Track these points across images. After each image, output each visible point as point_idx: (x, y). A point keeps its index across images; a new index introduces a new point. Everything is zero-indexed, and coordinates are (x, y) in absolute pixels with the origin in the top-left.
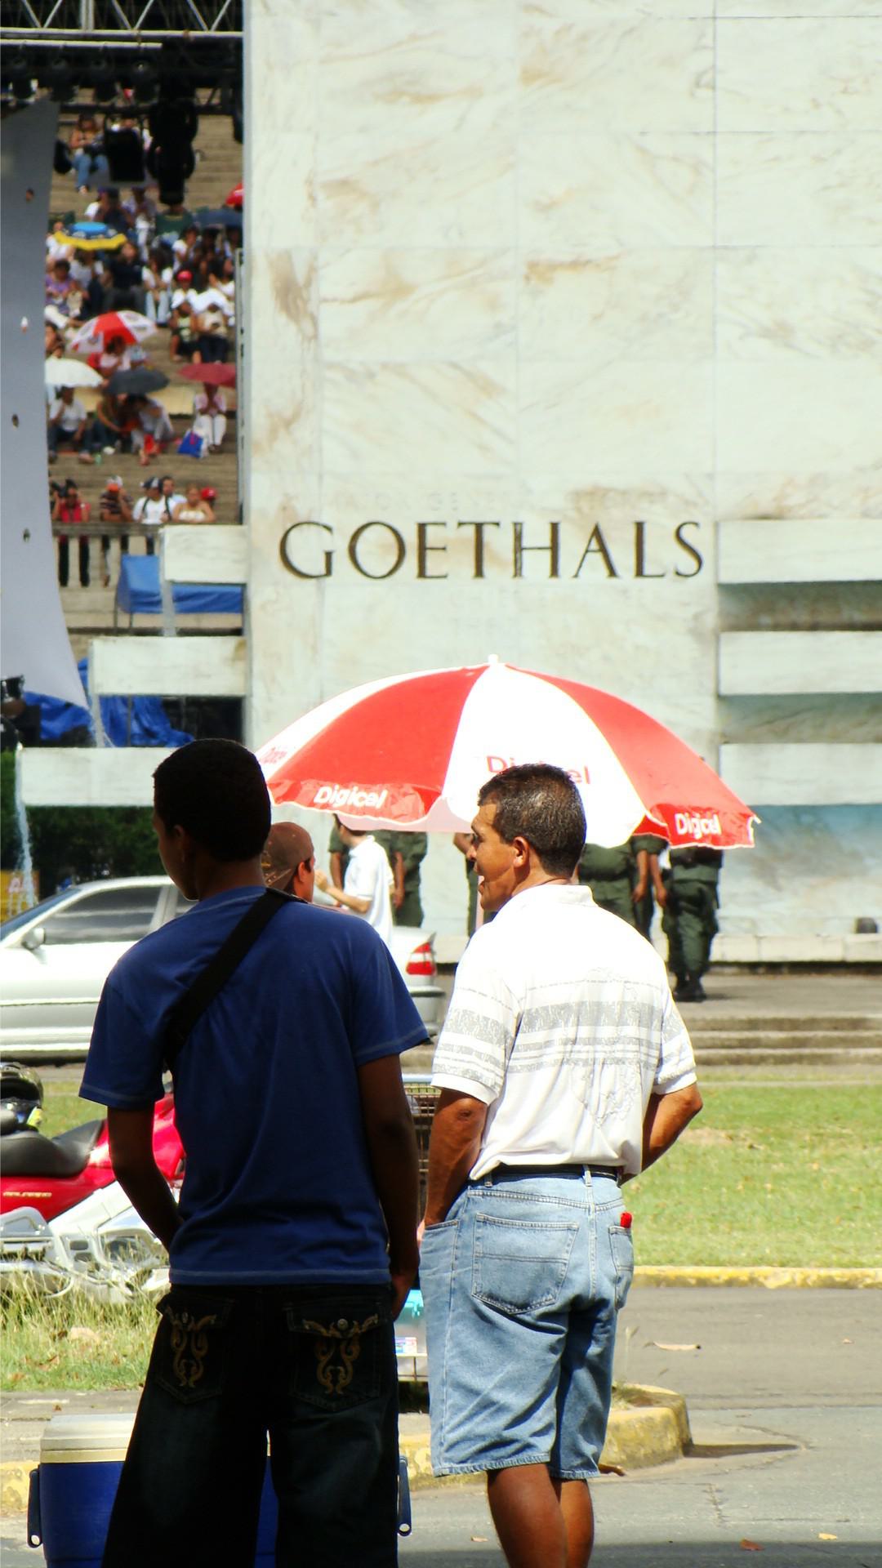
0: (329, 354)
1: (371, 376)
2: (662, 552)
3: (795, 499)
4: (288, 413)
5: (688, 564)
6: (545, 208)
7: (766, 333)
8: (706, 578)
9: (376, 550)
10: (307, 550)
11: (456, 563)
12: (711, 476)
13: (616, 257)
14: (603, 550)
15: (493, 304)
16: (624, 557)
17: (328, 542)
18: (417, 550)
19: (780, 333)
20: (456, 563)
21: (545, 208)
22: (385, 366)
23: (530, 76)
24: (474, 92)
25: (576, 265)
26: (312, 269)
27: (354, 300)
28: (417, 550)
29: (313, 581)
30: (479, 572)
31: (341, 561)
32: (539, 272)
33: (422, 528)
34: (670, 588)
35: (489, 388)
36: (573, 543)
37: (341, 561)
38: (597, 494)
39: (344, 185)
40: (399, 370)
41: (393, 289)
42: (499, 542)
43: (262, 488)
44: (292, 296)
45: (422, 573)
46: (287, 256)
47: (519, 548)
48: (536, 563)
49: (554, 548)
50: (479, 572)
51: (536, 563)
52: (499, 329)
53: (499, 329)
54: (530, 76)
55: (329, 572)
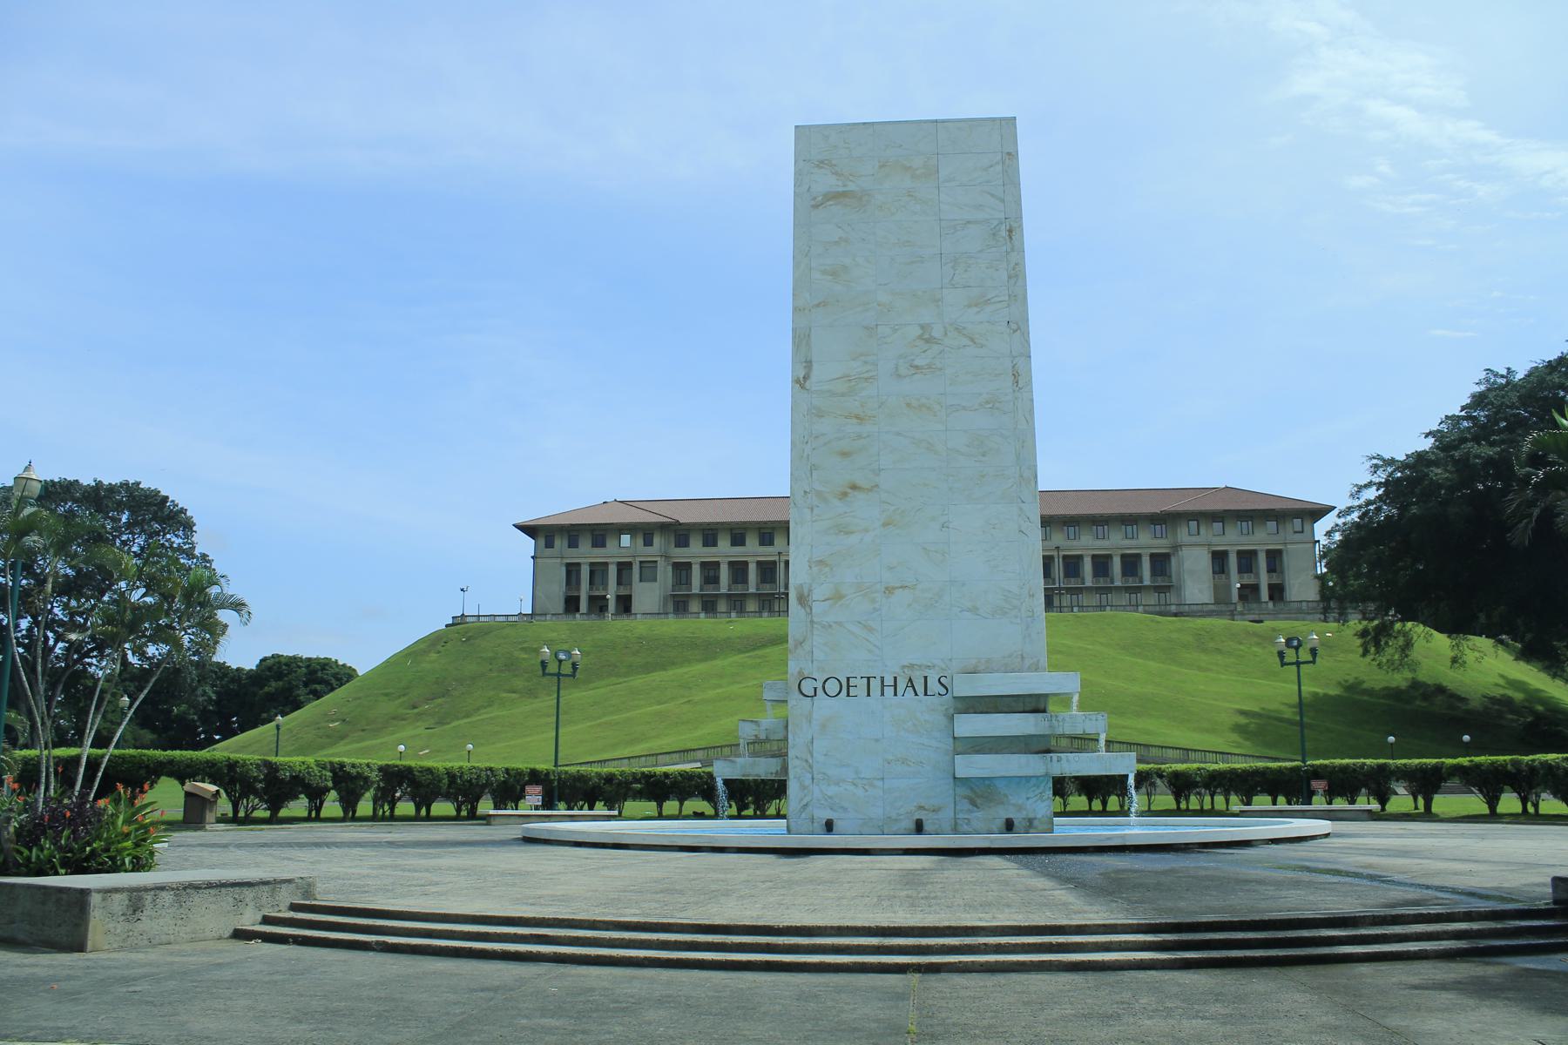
2: (934, 686)
3: (981, 668)
5: (943, 691)
6: (891, 568)
7: (969, 610)
9: (832, 687)
10: (807, 687)
15: (874, 601)
16: (920, 689)
17: (815, 684)
18: (847, 687)
19: (974, 610)
21: (891, 568)
23: (885, 525)
24: (866, 530)
28: (847, 687)
31: (820, 691)
32: (889, 590)
34: (936, 699)
35: (870, 630)
36: (901, 686)
37: (820, 691)
39: (821, 562)
40: (839, 624)
41: (837, 596)
42: (875, 684)
43: (793, 667)
44: (802, 600)
46: (801, 585)
47: (883, 686)
48: (889, 691)
49: (895, 686)
51: (889, 691)
53: (875, 610)
54: (885, 525)
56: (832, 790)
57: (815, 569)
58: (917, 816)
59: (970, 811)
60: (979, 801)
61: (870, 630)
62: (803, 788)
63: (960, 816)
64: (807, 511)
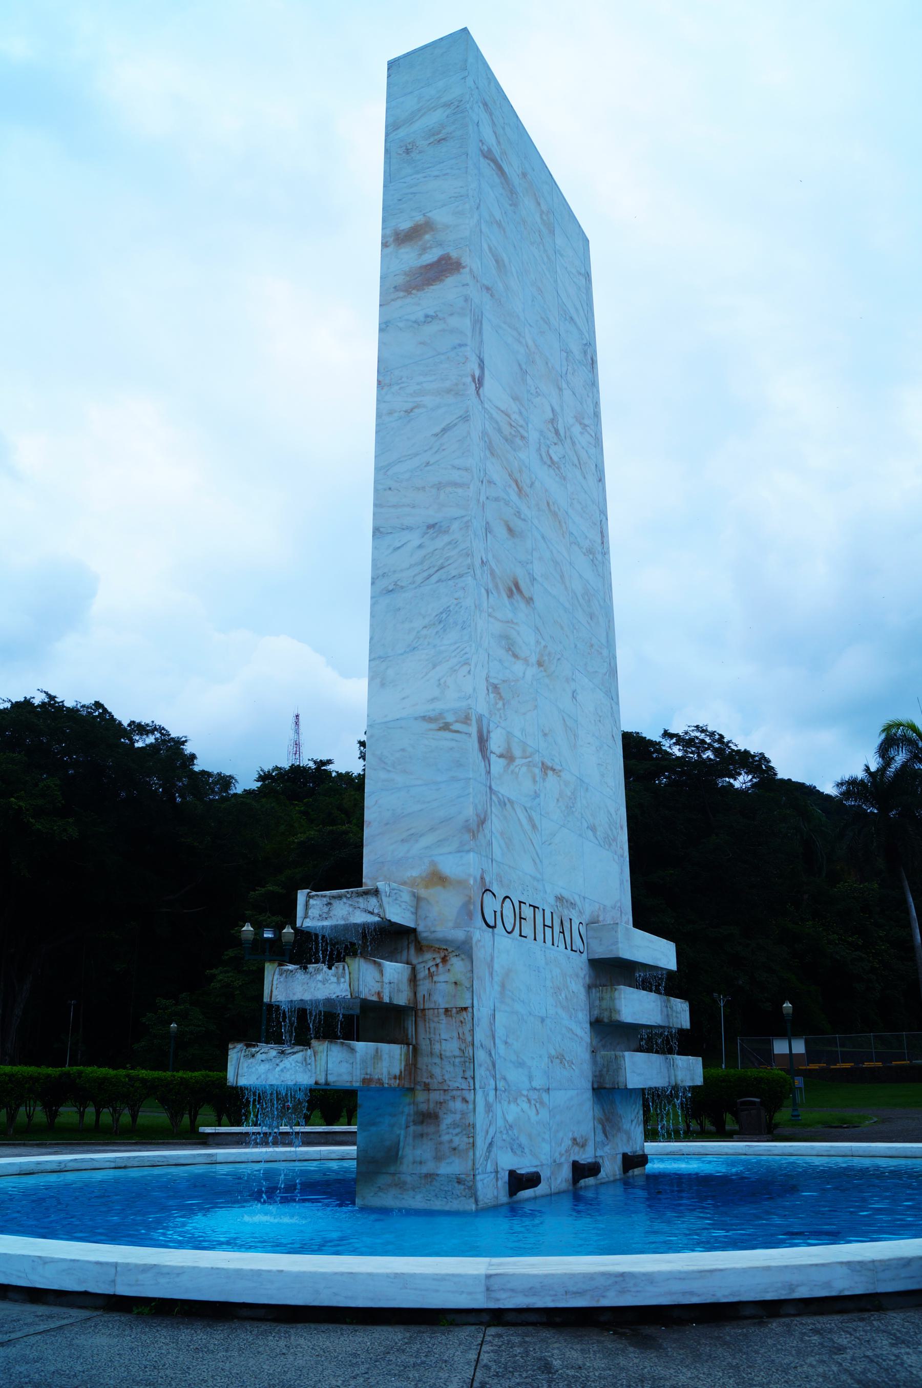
0: (494, 787)
1: (505, 804)
4: (482, 817)
6: (545, 735)
8: (585, 955)
11: (527, 930)
12: (584, 898)
13: (560, 771)
14: (563, 932)
20: (527, 930)
22: (509, 800)
24: (526, 660)
25: (553, 770)
26: (489, 732)
27: (501, 756)
29: (491, 930)
30: (535, 939)
33: (520, 902)
35: (534, 826)
38: (560, 899)
39: (495, 687)
40: (511, 802)
45: (521, 935)
47: (544, 925)
49: (552, 927)
50: (535, 939)
52: (537, 795)
55: (495, 927)
56: (512, 1112)
57: (492, 696)
58: (572, 1158)
59: (604, 1145)
60: (607, 1128)
61: (534, 826)
62: (489, 1108)
63: (599, 1153)
64: (483, 591)
